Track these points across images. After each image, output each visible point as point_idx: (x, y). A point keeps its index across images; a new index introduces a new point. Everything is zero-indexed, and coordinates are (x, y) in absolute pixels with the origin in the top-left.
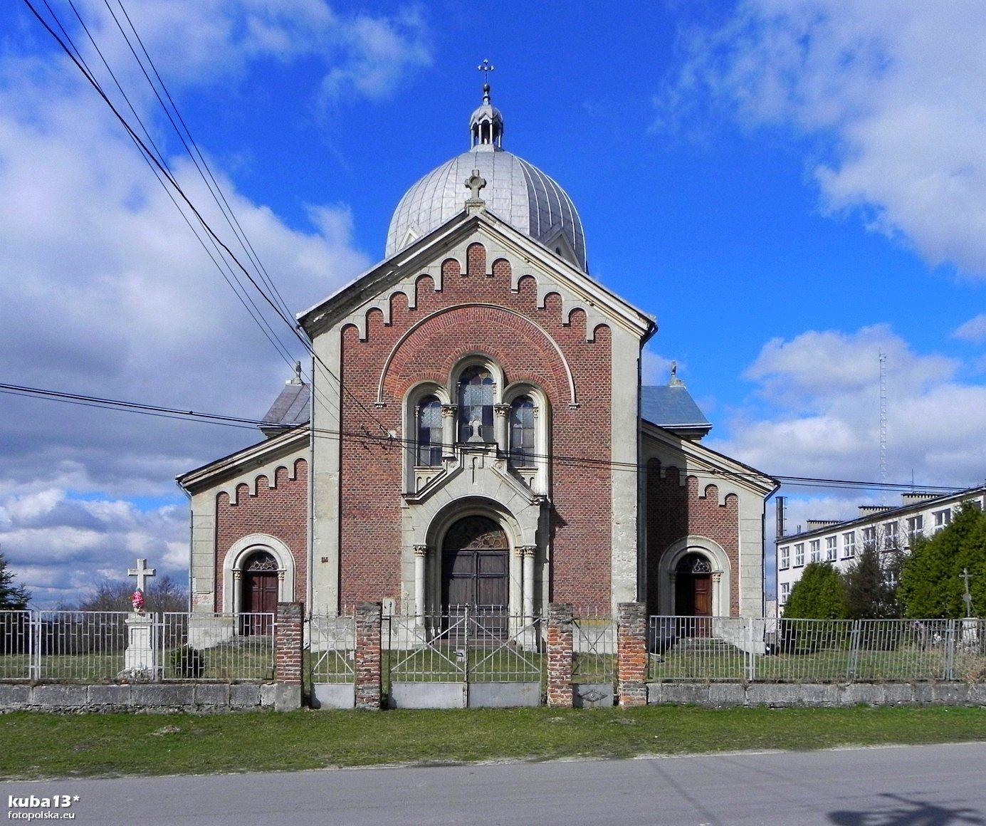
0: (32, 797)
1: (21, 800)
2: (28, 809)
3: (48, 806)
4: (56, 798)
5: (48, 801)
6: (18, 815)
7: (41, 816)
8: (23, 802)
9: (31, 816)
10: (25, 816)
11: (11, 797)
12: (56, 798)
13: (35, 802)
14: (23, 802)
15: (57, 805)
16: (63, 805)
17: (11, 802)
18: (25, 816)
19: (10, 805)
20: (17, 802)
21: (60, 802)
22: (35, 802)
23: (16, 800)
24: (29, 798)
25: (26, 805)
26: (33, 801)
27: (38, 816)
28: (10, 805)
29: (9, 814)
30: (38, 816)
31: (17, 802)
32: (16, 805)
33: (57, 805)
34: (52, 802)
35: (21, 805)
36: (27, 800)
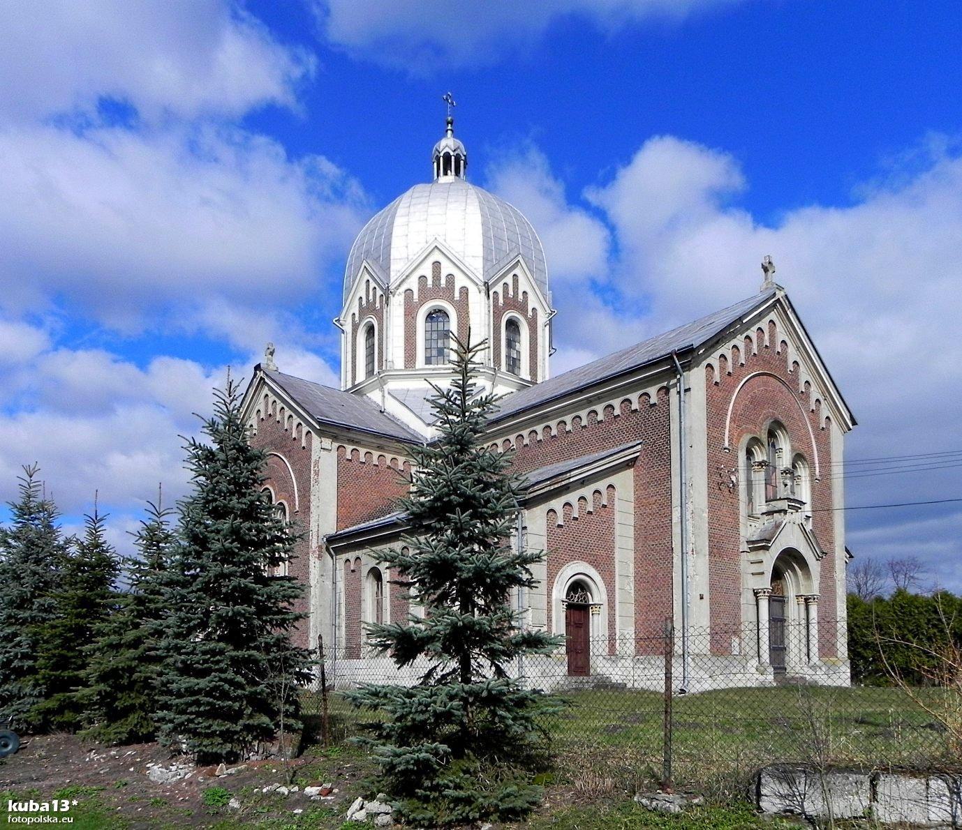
0: (31, 801)
1: (20, 804)
2: (23, 814)
3: (47, 810)
4: (55, 802)
5: (47, 805)
6: (18, 819)
7: (40, 820)
8: (23, 806)
9: (31, 820)
10: (24, 820)
11: (11, 802)
12: (55, 802)
13: (34, 807)
14: (23, 806)
15: (55, 809)
16: (62, 810)
17: (11, 807)
18: (24, 820)
19: (10, 810)
20: (17, 806)
21: (60, 806)
22: (34, 807)
23: (15, 804)
24: (28, 802)
25: (25, 809)
26: (32, 806)
27: (37, 820)
28: (10, 810)
29: (9, 818)
30: (37, 820)
31: (17, 806)
32: (15, 810)
33: (55, 809)
34: (51, 807)
35: (21, 809)
36: (26, 804)
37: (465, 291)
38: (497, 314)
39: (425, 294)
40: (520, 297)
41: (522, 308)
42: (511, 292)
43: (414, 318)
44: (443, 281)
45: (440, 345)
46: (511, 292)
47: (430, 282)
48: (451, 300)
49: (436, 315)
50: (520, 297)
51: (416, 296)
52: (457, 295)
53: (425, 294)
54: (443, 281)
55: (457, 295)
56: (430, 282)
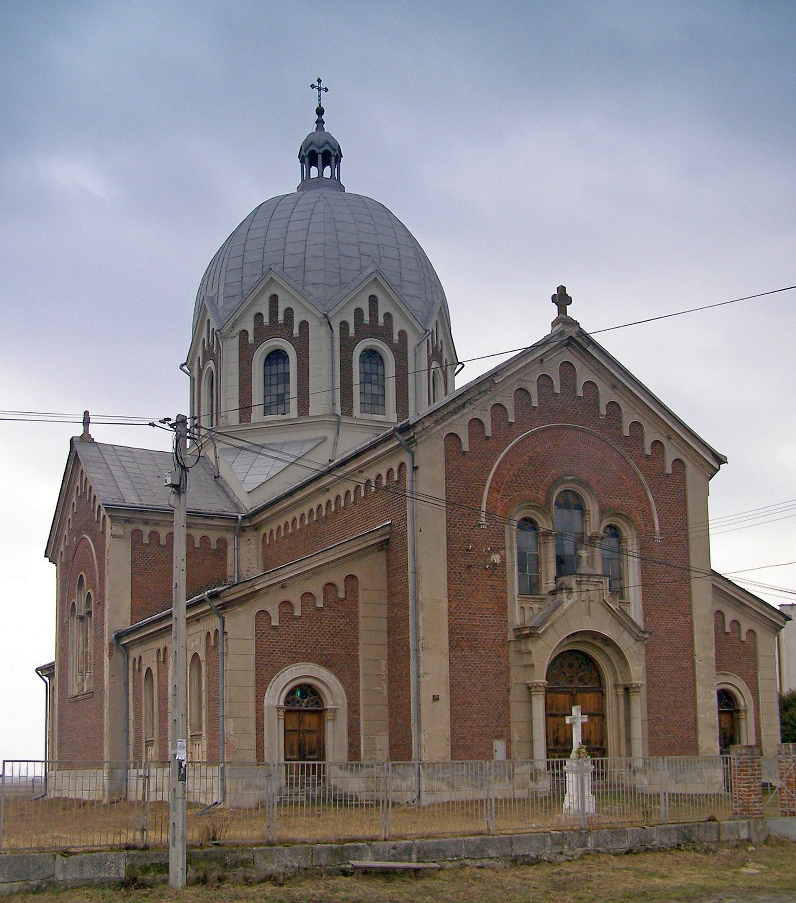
37: (304, 325)
38: (347, 346)
39: (262, 333)
40: (381, 321)
41: (385, 334)
42: (367, 318)
43: (250, 363)
44: (281, 318)
45: (281, 391)
46: (367, 318)
47: (266, 320)
48: (290, 338)
49: (276, 357)
50: (381, 321)
51: (251, 338)
52: (296, 331)
53: (262, 333)
54: (281, 318)
55: (296, 331)
56: (266, 320)
